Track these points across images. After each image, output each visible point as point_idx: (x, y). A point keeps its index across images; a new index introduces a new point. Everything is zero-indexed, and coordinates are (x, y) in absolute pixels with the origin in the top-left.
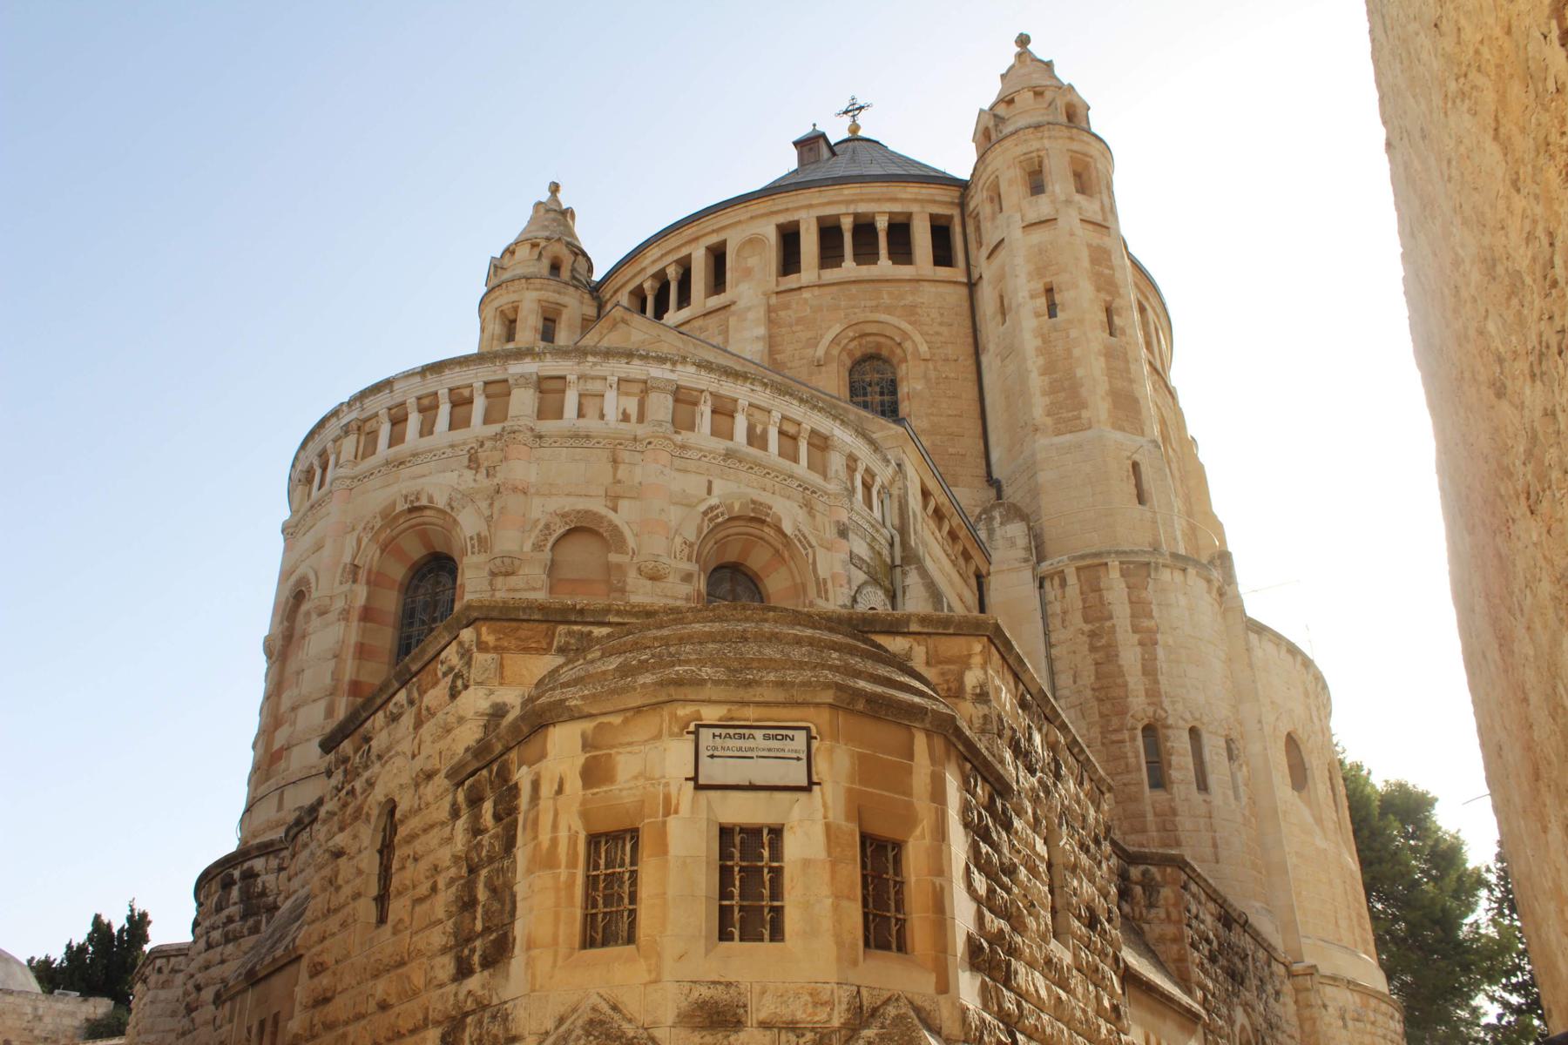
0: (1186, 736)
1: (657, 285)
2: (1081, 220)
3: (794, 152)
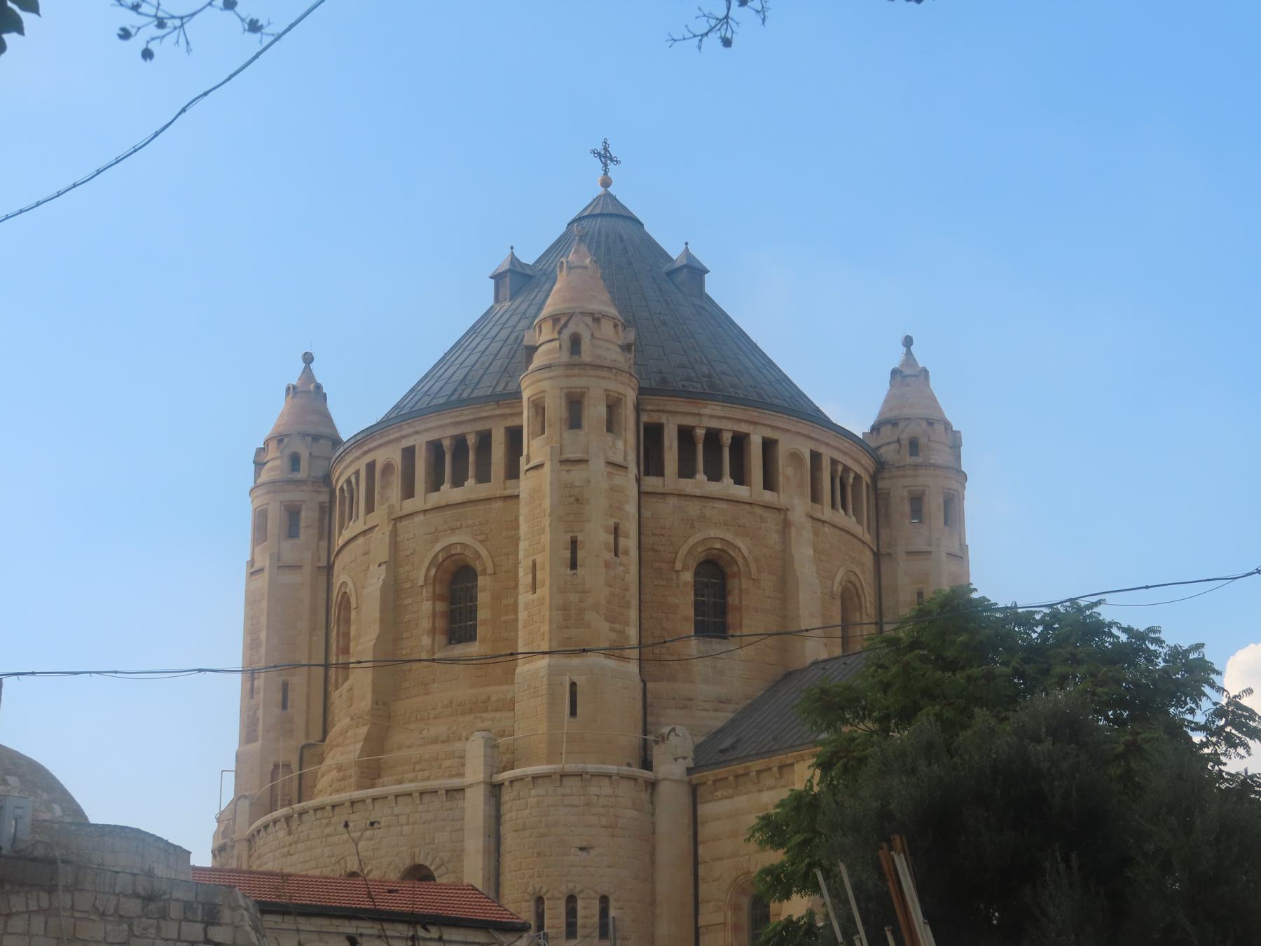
2: (560, 462)
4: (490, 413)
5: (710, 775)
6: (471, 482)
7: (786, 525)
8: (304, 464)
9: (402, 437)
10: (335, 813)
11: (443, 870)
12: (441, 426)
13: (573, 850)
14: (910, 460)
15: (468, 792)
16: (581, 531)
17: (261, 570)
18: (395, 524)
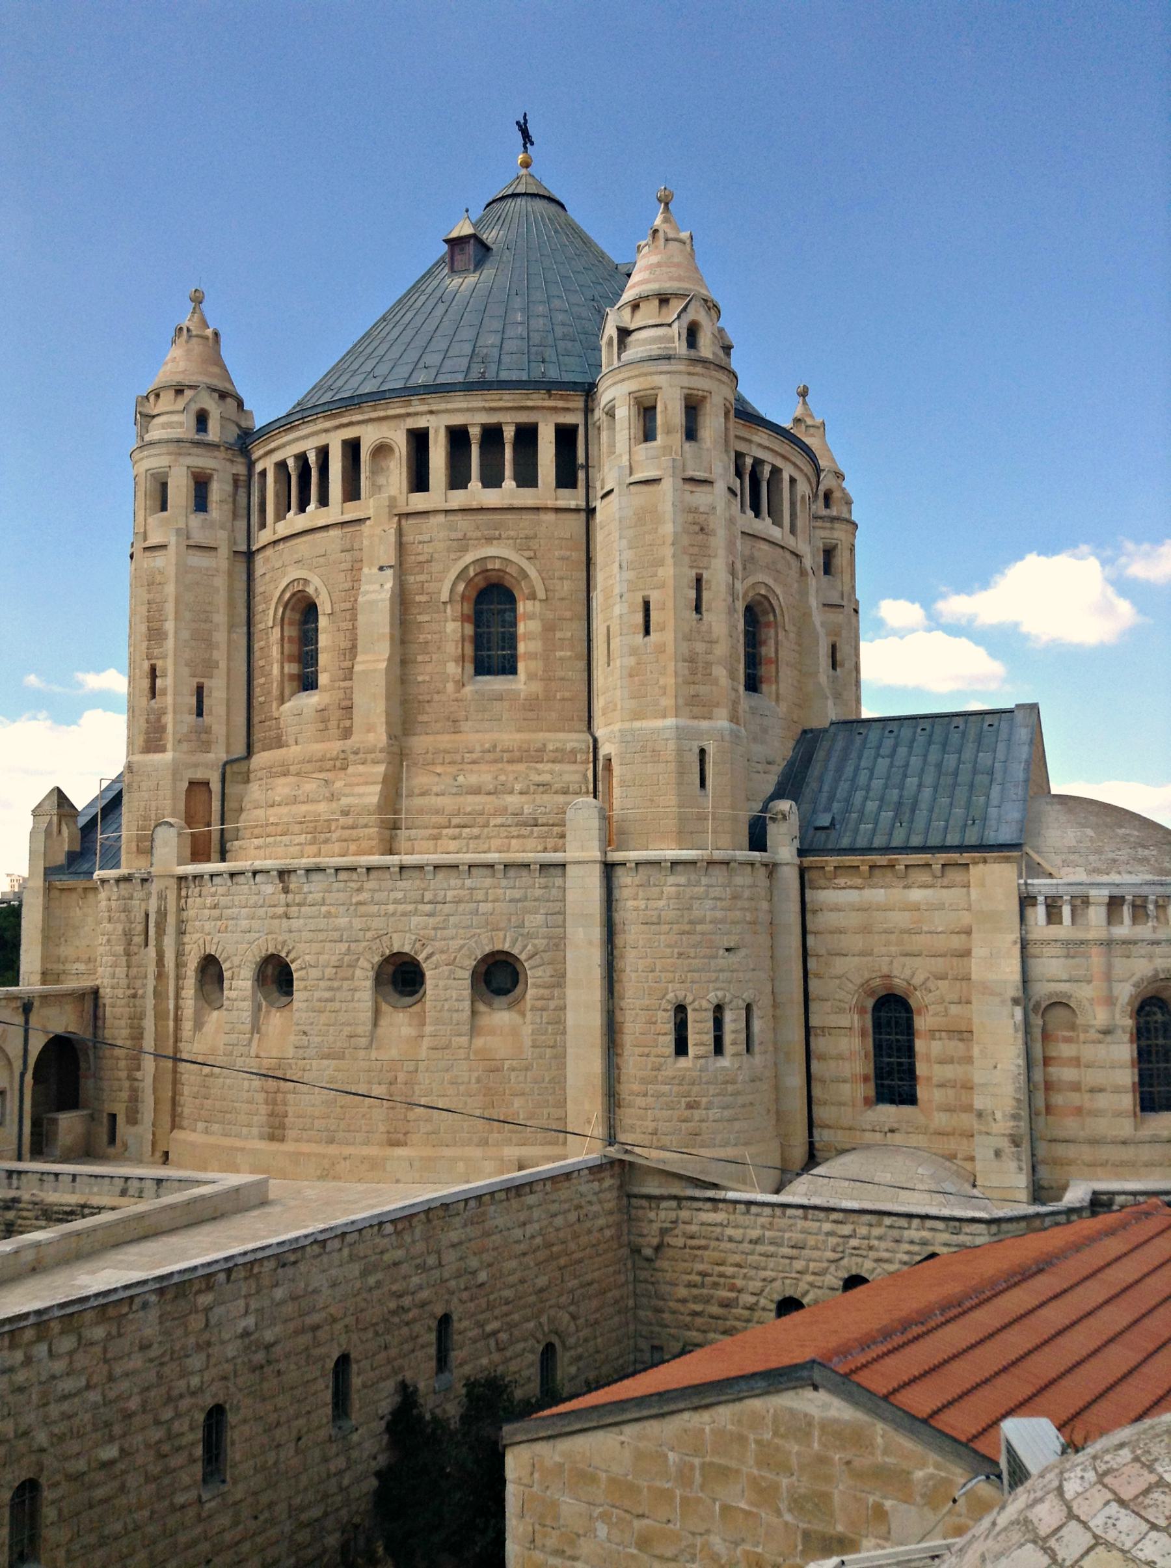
0: (710, 1015)
1: (301, 463)
3: (445, 248)
4: (540, 403)
5: (833, 861)
6: (509, 483)
7: (803, 573)
8: (213, 424)
9: (409, 415)
10: (371, 877)
11: (537, 960)
12: (468, 410)
13: (721, 952)
14: (824, 512)
15: (568, 867)
16: (706, 568)
17: (163, 547)
18: (399, 521)
